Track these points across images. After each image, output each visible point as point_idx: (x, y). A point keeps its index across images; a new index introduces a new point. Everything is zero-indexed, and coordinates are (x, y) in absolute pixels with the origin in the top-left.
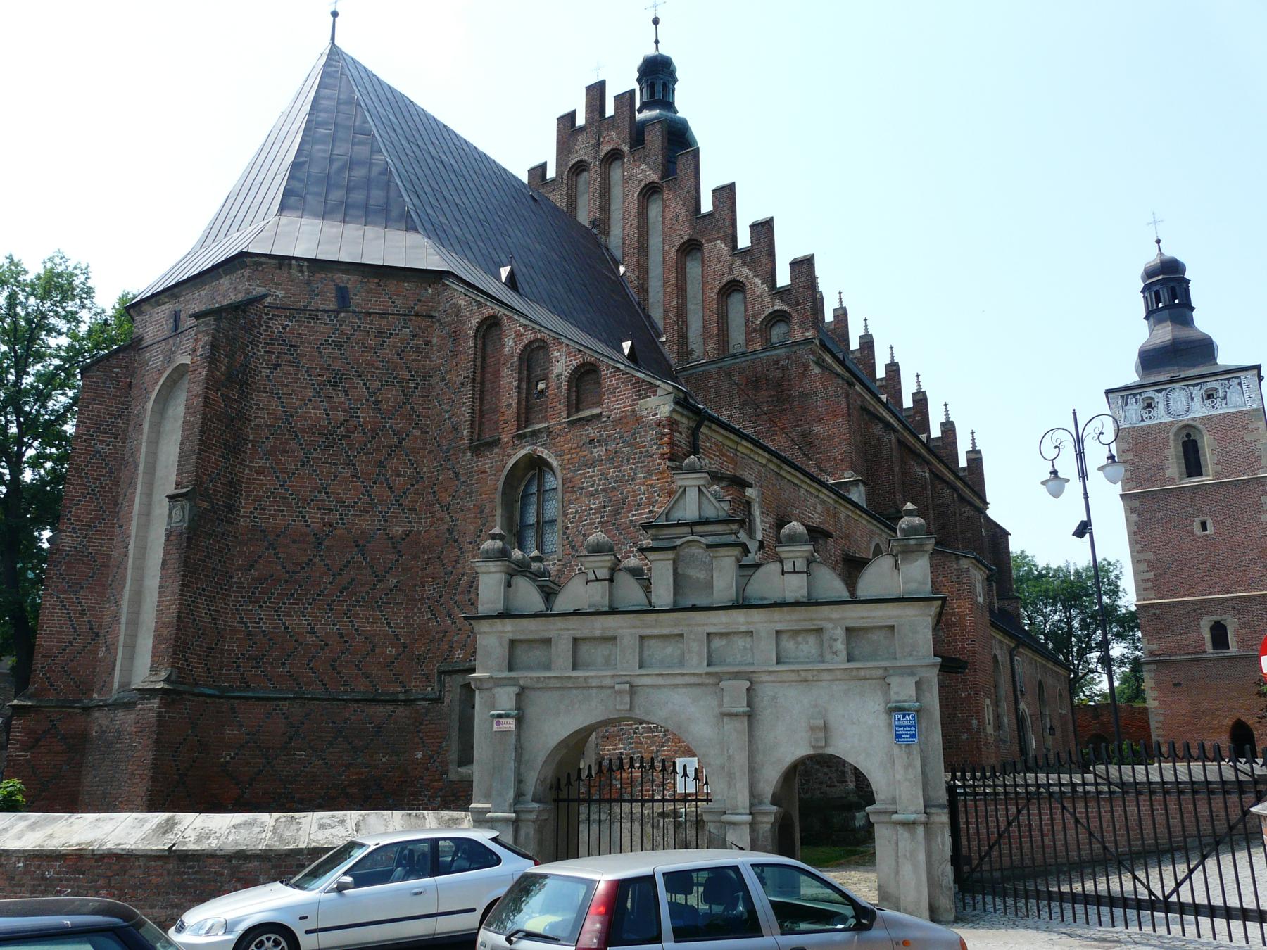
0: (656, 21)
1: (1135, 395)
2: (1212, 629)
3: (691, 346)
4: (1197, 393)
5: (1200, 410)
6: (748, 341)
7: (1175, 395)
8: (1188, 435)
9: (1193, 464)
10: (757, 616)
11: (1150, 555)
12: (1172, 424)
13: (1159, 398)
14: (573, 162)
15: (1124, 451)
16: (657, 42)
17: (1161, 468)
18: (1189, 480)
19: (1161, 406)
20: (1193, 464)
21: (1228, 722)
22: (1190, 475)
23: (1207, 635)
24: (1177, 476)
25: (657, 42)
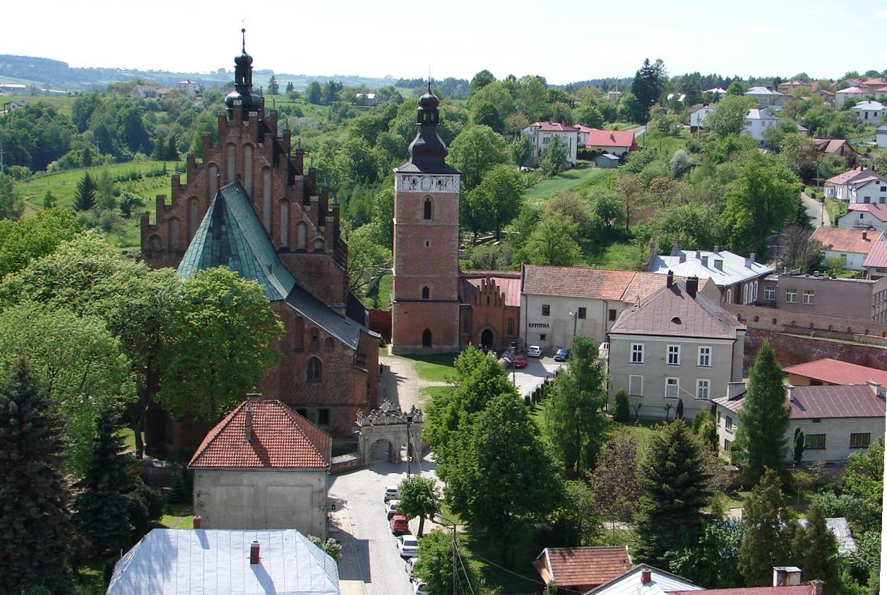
0: (243, 31)
1: (409, 176)
2: (423, 289)
3: (282, 241)
4: (435, 180)
5: (435, 189)
6: (307, 247)
7: (425, 179)
8: (428, 199)
9: (428, 213)
10: (401, 425)
11: (404, 254)
12: (422, 193)
13: (419, 179)
14: (227, 142)
15: (400, 203)
16: (244, 44)
17: (414, 214)
18: (424, 221)
19: (419, 184)
20: (428, 213)
21: (423, 329)
22: (426, 218)
23: (421, 293)
24: (420, 219)
25: (244, 44)
